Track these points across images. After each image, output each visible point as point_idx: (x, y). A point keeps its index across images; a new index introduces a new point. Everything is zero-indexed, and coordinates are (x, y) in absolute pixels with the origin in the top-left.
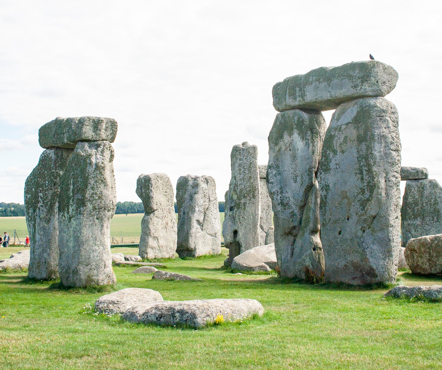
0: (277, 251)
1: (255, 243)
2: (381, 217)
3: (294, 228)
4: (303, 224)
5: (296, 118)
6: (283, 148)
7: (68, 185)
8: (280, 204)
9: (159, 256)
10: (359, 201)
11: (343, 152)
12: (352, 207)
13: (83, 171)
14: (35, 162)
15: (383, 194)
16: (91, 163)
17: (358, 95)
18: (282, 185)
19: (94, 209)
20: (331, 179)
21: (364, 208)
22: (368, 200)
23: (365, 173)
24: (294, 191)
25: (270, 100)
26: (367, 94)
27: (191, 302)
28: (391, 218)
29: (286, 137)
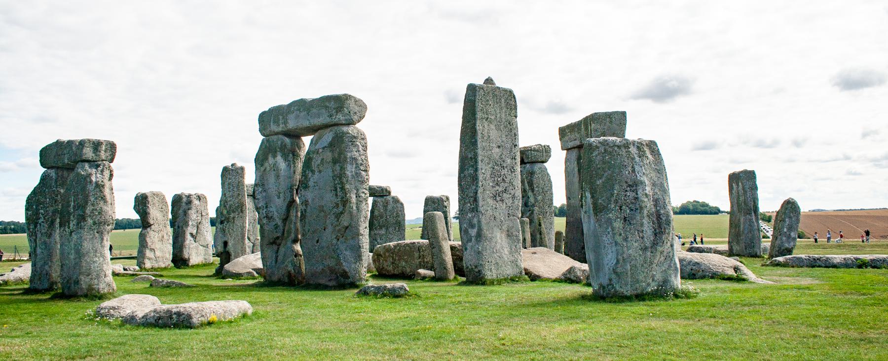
0: (263, 259)
1: (243, 252)
3: (278, 238)
6: (268, 168)
7: (68, 202)
8: (265, 218)
9: (156, 266)
11: (320, 172)
13: (84, 189)
14: (37, 182)
15: (354, 208)
16: (91, 181)
19: (95, 223)
20: (309, 195)
22: (342, 213)
23: (339, 189)
24: (278, 205)
25: (257, 126)
27: (187, 305)
28: (361, 228)
29: (271, 160)
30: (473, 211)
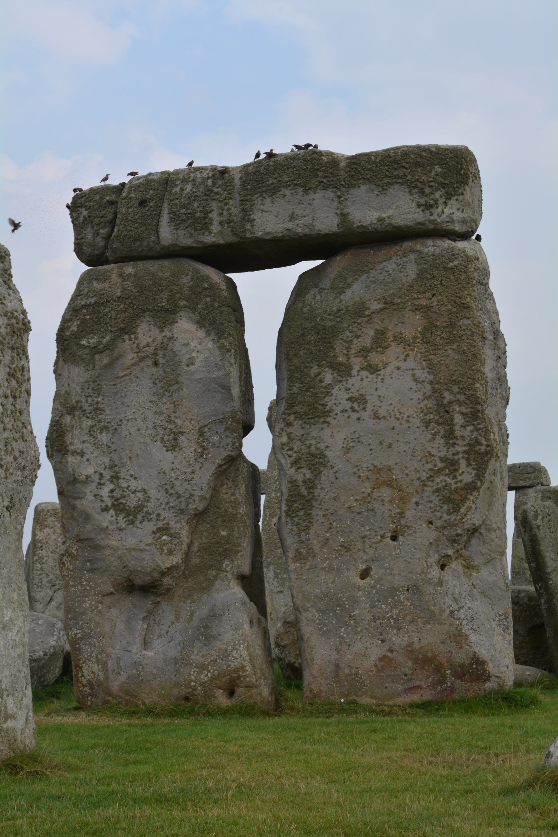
2: (489, 530)
4: (195, 560)
5: (186, 281)
6: (130, 357)
10: (437, 490)
11: (372, 369)
12: (412, 505)
17: (431, 227)
18: (116, 458)
21: (456, 510)
22: (471, 488)
23: (458, 419)
26: (450, 227)
29: (147, 333)
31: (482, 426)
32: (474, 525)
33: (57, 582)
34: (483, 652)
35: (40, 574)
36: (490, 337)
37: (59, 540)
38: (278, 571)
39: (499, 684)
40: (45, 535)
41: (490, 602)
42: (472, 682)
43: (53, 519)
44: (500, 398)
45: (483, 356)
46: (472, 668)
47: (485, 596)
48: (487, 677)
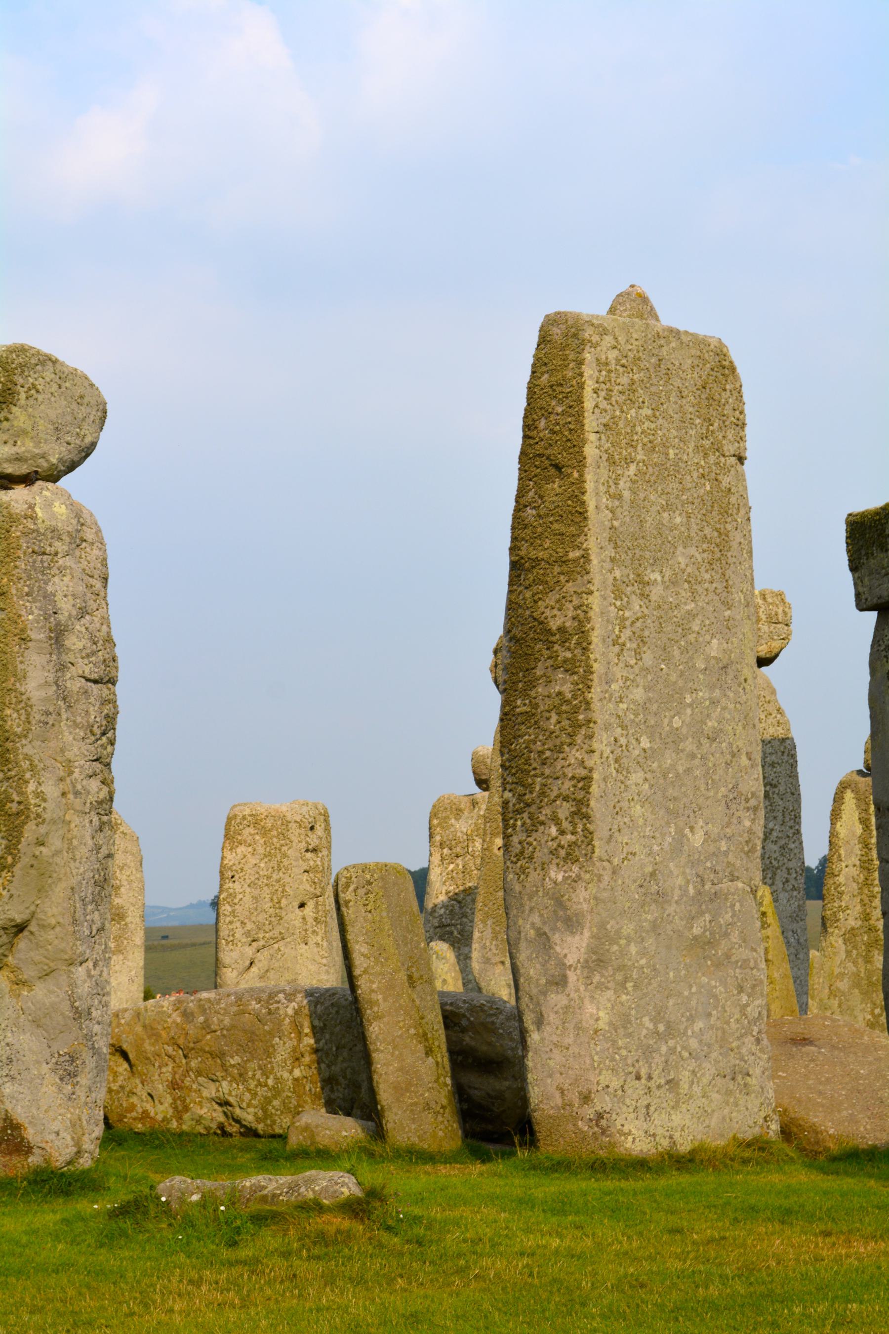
2: (43, 927)
30: (571, 858)
31: (13, 773)
32: (12, 920)
33: (261, 936)
34: (19, 1110)
35: (231, 922)
36: (38, 635)
37: (262, 865)
38: (498, 929)
39: (45, 1159)
40: (240, 856)
41: (46, 1034)
42: (10, 1154)
43: (252, 830)
44: (69, 727)
45: (20, 667)
46: (7, 1135)
47: (38, 1026)
48: (29, 1150)
